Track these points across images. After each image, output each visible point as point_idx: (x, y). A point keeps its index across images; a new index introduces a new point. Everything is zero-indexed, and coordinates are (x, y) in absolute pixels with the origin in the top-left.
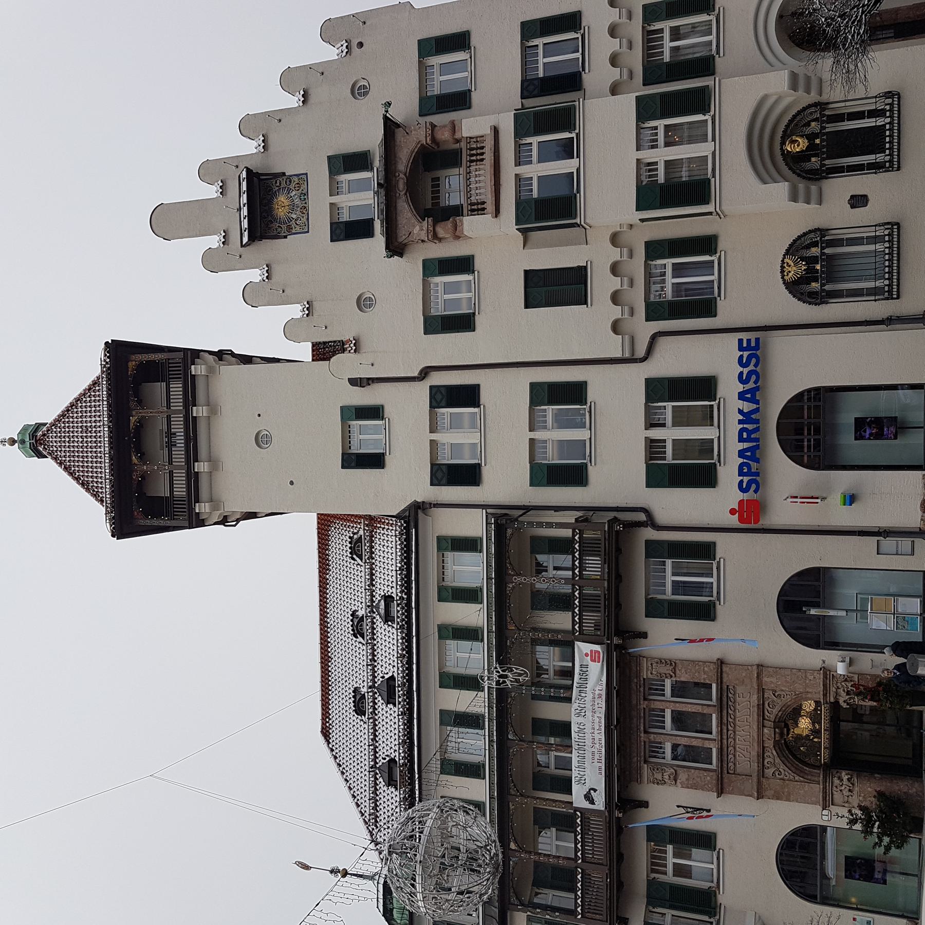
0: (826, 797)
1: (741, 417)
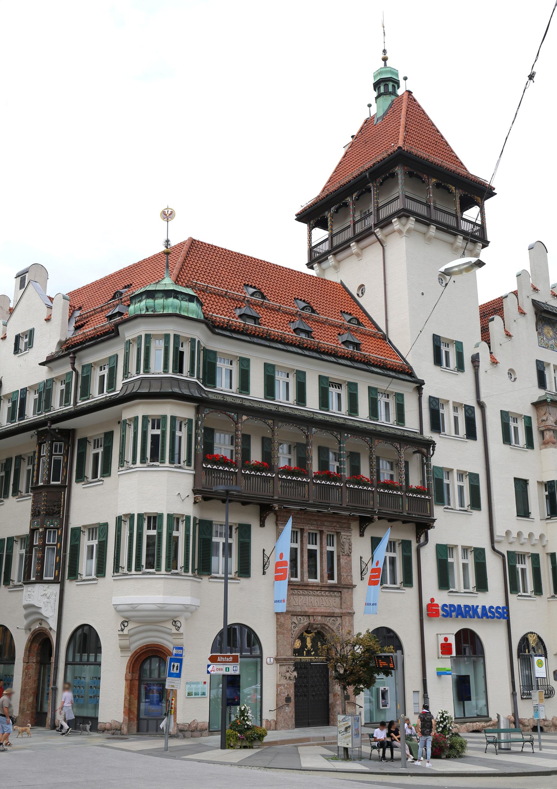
0: (285, 661)
1: (475, 607)
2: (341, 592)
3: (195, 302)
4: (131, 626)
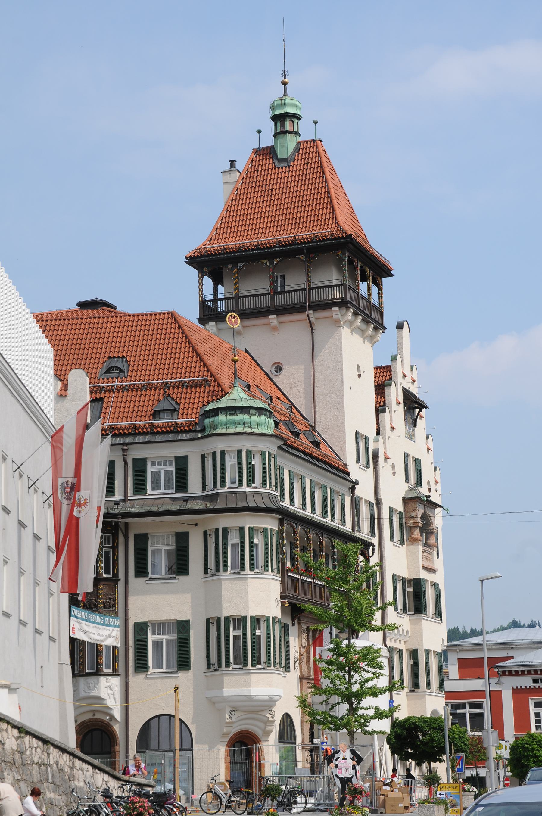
4: (238, 714)
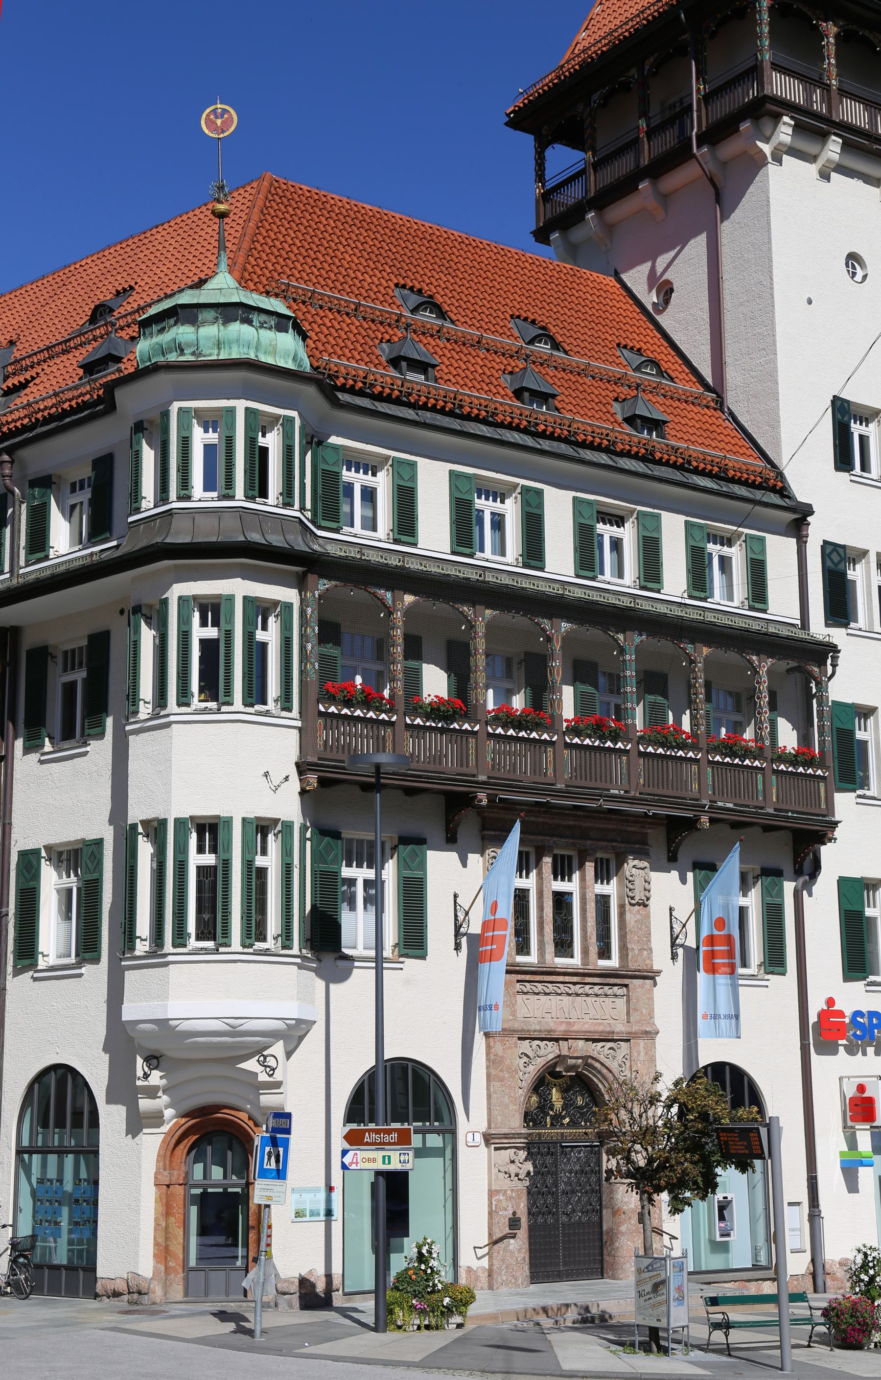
0: (506, 1138)
2: (626, 986)
3: (291, 330)
